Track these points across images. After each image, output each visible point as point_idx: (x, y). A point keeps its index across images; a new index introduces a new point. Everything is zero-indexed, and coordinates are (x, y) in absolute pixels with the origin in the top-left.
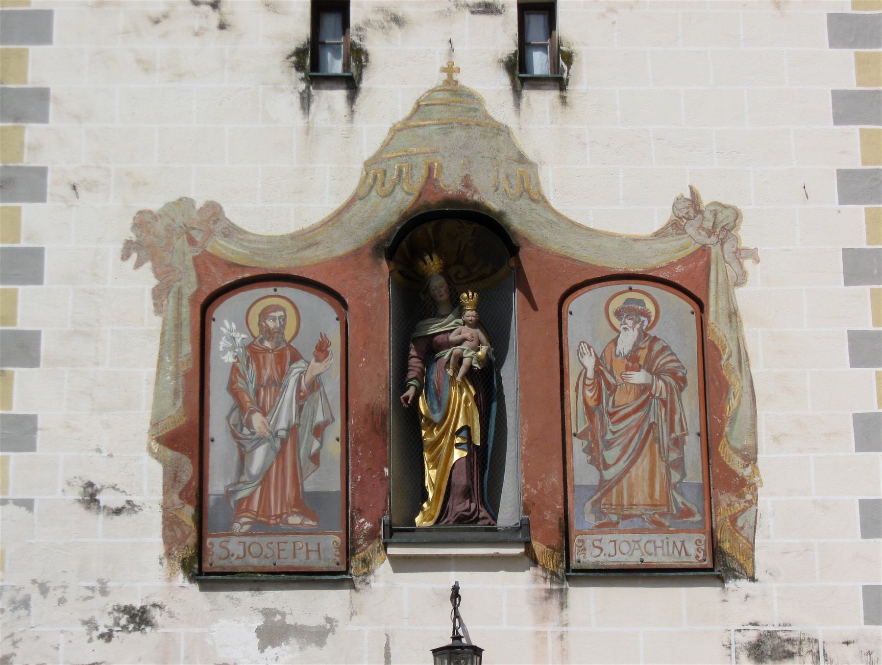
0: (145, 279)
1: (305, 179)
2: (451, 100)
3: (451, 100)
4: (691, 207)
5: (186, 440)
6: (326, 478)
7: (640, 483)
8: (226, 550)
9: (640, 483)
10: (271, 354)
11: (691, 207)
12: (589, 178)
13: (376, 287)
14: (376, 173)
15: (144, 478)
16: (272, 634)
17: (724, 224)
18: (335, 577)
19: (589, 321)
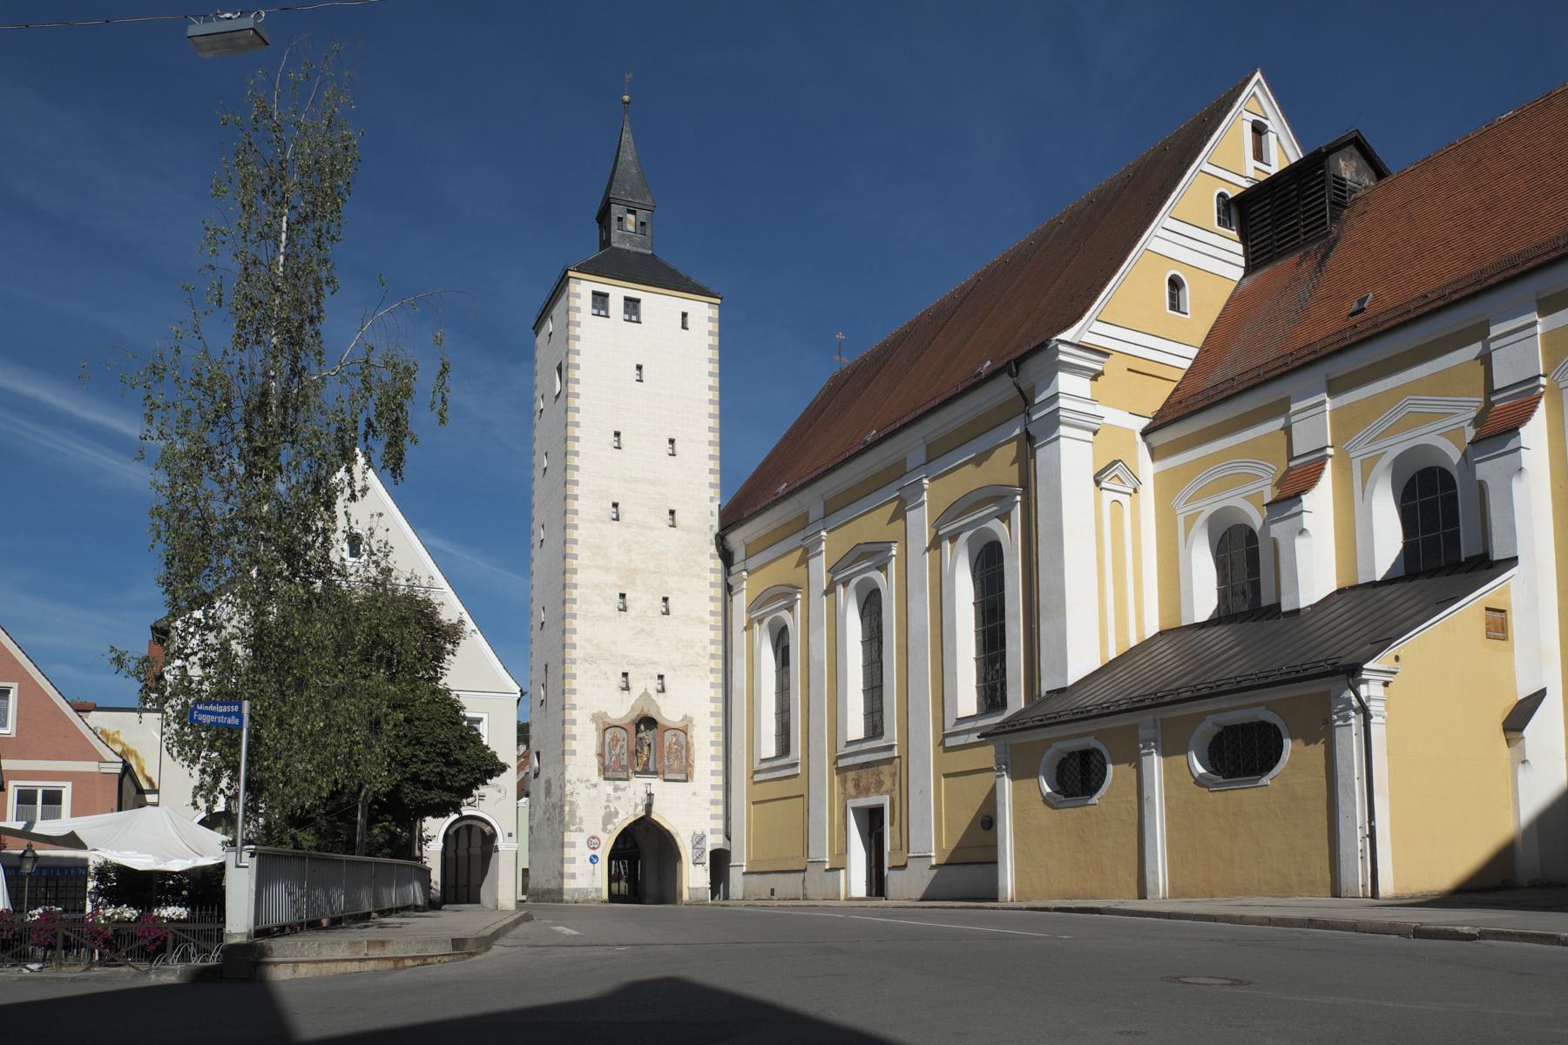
0: (594, 726)
1: (621, 709)
2: (646, 694)
3: (646, 694)
4: (685, 717)
5: (601, 755)
6: (624, 762)
7: (676, 765)
8: (609, 774)
9: (676, 765)
10: (615, 740)
11: (685, 717)
12: (669, 711)
13: (633, 729)
14: (633, 708)
15: (594, 762)
16: (616, 789)
17: (691, 720)
18: (627, 779)
19: (669, 738)
